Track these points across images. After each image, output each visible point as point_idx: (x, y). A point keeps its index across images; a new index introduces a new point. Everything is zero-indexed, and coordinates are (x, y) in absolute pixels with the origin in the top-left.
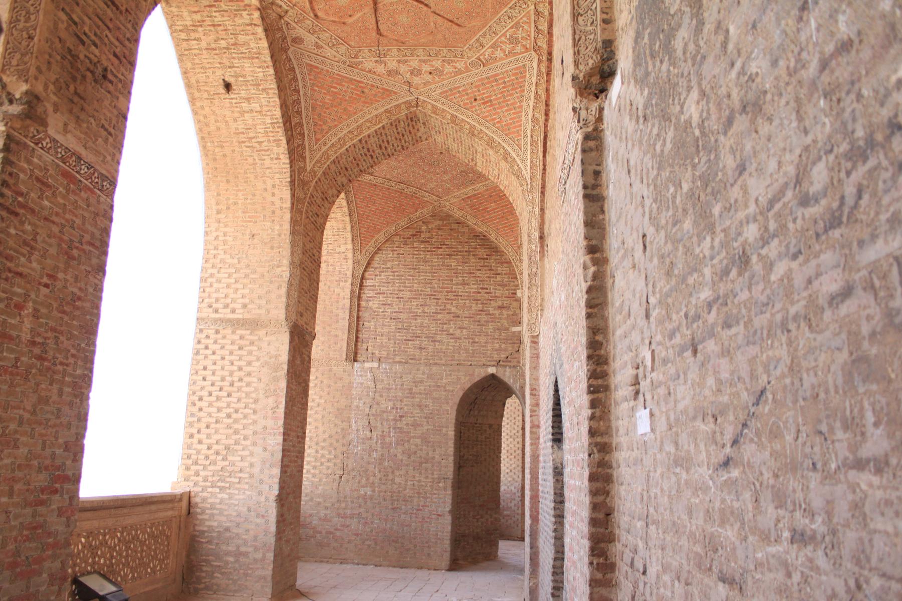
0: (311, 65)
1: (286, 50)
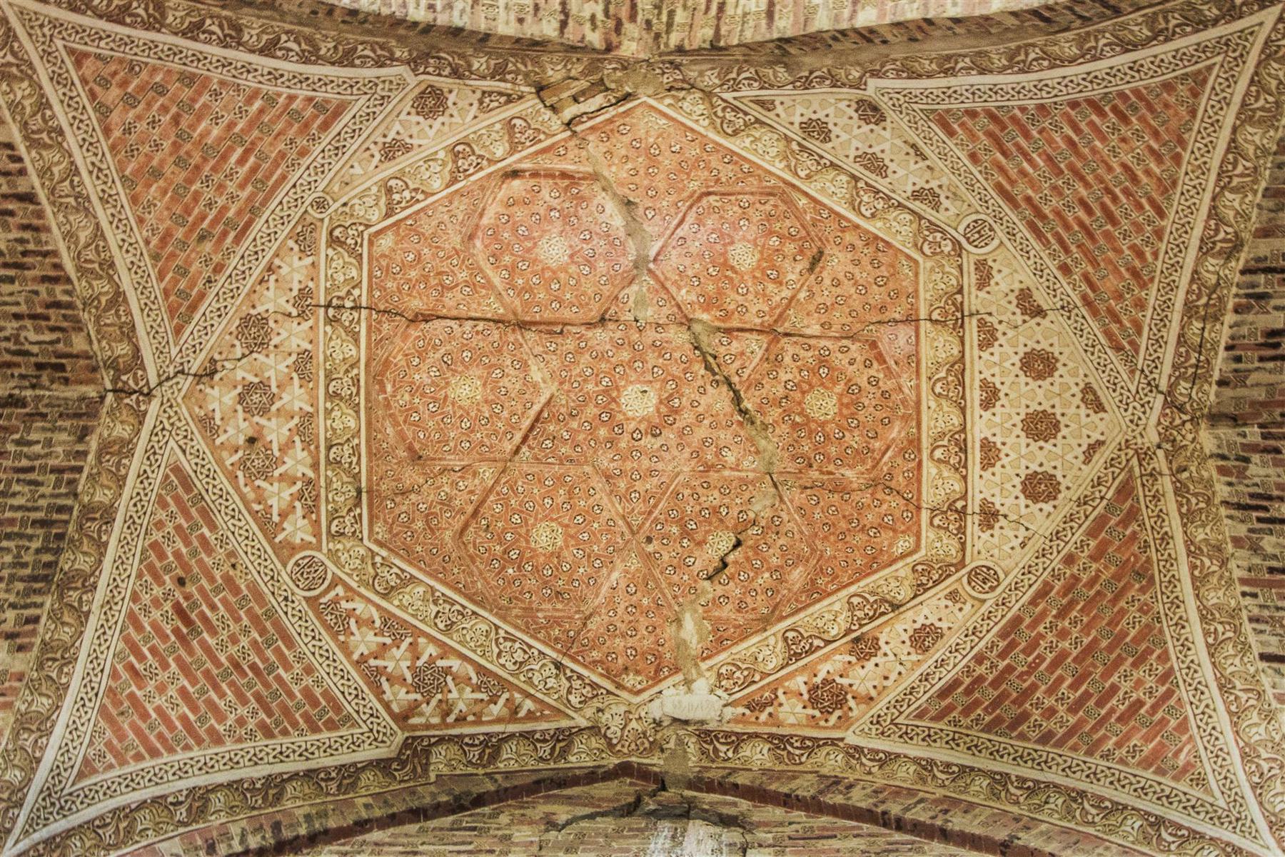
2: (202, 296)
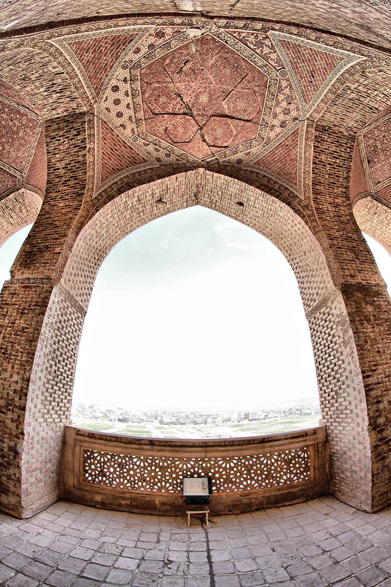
0: (256, 162)
1: (240, 169)
2: (291, 134)
